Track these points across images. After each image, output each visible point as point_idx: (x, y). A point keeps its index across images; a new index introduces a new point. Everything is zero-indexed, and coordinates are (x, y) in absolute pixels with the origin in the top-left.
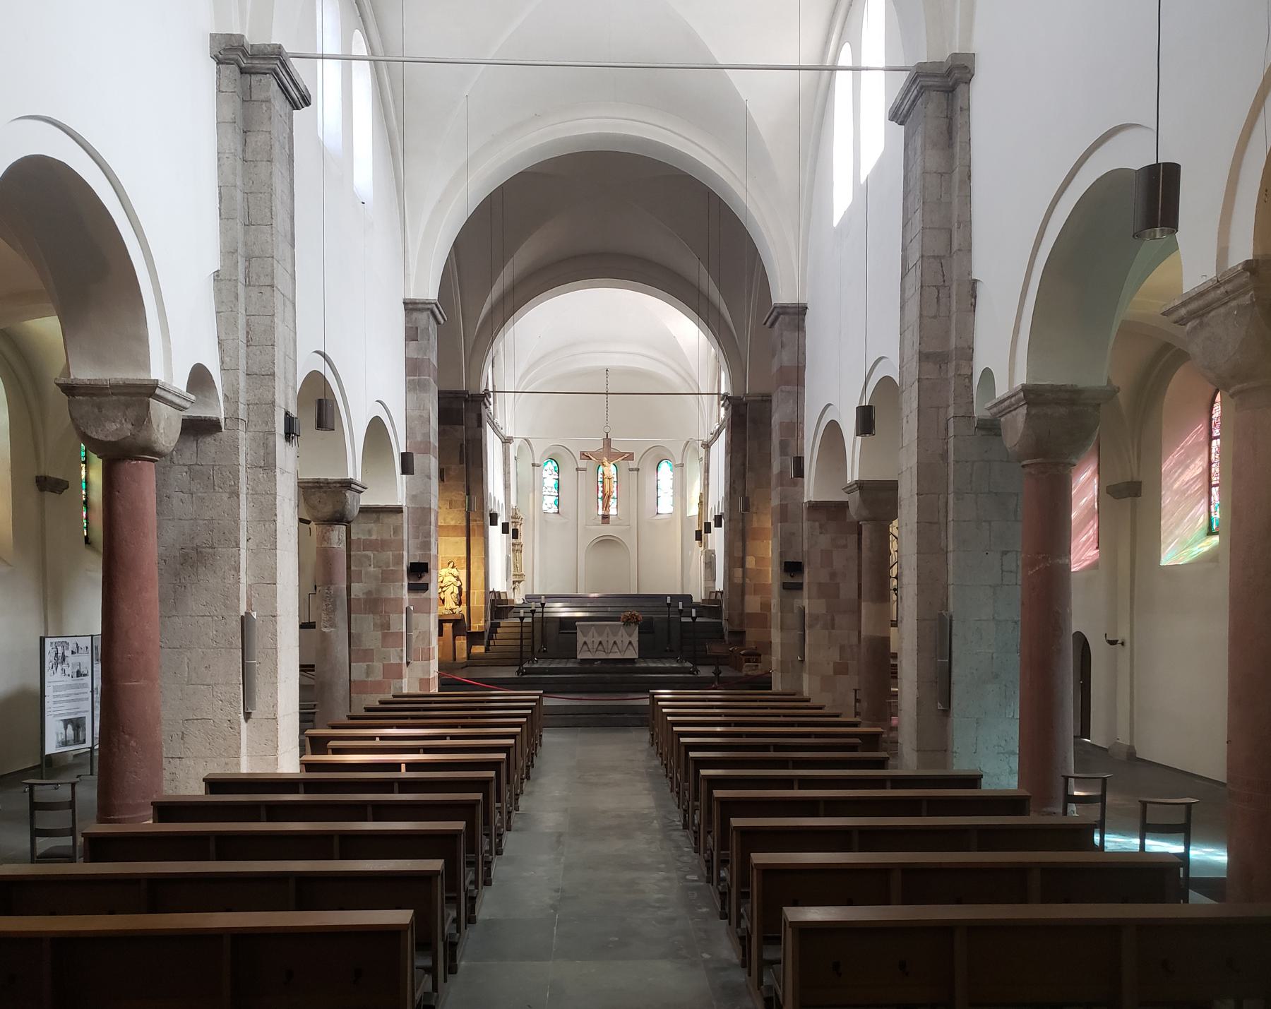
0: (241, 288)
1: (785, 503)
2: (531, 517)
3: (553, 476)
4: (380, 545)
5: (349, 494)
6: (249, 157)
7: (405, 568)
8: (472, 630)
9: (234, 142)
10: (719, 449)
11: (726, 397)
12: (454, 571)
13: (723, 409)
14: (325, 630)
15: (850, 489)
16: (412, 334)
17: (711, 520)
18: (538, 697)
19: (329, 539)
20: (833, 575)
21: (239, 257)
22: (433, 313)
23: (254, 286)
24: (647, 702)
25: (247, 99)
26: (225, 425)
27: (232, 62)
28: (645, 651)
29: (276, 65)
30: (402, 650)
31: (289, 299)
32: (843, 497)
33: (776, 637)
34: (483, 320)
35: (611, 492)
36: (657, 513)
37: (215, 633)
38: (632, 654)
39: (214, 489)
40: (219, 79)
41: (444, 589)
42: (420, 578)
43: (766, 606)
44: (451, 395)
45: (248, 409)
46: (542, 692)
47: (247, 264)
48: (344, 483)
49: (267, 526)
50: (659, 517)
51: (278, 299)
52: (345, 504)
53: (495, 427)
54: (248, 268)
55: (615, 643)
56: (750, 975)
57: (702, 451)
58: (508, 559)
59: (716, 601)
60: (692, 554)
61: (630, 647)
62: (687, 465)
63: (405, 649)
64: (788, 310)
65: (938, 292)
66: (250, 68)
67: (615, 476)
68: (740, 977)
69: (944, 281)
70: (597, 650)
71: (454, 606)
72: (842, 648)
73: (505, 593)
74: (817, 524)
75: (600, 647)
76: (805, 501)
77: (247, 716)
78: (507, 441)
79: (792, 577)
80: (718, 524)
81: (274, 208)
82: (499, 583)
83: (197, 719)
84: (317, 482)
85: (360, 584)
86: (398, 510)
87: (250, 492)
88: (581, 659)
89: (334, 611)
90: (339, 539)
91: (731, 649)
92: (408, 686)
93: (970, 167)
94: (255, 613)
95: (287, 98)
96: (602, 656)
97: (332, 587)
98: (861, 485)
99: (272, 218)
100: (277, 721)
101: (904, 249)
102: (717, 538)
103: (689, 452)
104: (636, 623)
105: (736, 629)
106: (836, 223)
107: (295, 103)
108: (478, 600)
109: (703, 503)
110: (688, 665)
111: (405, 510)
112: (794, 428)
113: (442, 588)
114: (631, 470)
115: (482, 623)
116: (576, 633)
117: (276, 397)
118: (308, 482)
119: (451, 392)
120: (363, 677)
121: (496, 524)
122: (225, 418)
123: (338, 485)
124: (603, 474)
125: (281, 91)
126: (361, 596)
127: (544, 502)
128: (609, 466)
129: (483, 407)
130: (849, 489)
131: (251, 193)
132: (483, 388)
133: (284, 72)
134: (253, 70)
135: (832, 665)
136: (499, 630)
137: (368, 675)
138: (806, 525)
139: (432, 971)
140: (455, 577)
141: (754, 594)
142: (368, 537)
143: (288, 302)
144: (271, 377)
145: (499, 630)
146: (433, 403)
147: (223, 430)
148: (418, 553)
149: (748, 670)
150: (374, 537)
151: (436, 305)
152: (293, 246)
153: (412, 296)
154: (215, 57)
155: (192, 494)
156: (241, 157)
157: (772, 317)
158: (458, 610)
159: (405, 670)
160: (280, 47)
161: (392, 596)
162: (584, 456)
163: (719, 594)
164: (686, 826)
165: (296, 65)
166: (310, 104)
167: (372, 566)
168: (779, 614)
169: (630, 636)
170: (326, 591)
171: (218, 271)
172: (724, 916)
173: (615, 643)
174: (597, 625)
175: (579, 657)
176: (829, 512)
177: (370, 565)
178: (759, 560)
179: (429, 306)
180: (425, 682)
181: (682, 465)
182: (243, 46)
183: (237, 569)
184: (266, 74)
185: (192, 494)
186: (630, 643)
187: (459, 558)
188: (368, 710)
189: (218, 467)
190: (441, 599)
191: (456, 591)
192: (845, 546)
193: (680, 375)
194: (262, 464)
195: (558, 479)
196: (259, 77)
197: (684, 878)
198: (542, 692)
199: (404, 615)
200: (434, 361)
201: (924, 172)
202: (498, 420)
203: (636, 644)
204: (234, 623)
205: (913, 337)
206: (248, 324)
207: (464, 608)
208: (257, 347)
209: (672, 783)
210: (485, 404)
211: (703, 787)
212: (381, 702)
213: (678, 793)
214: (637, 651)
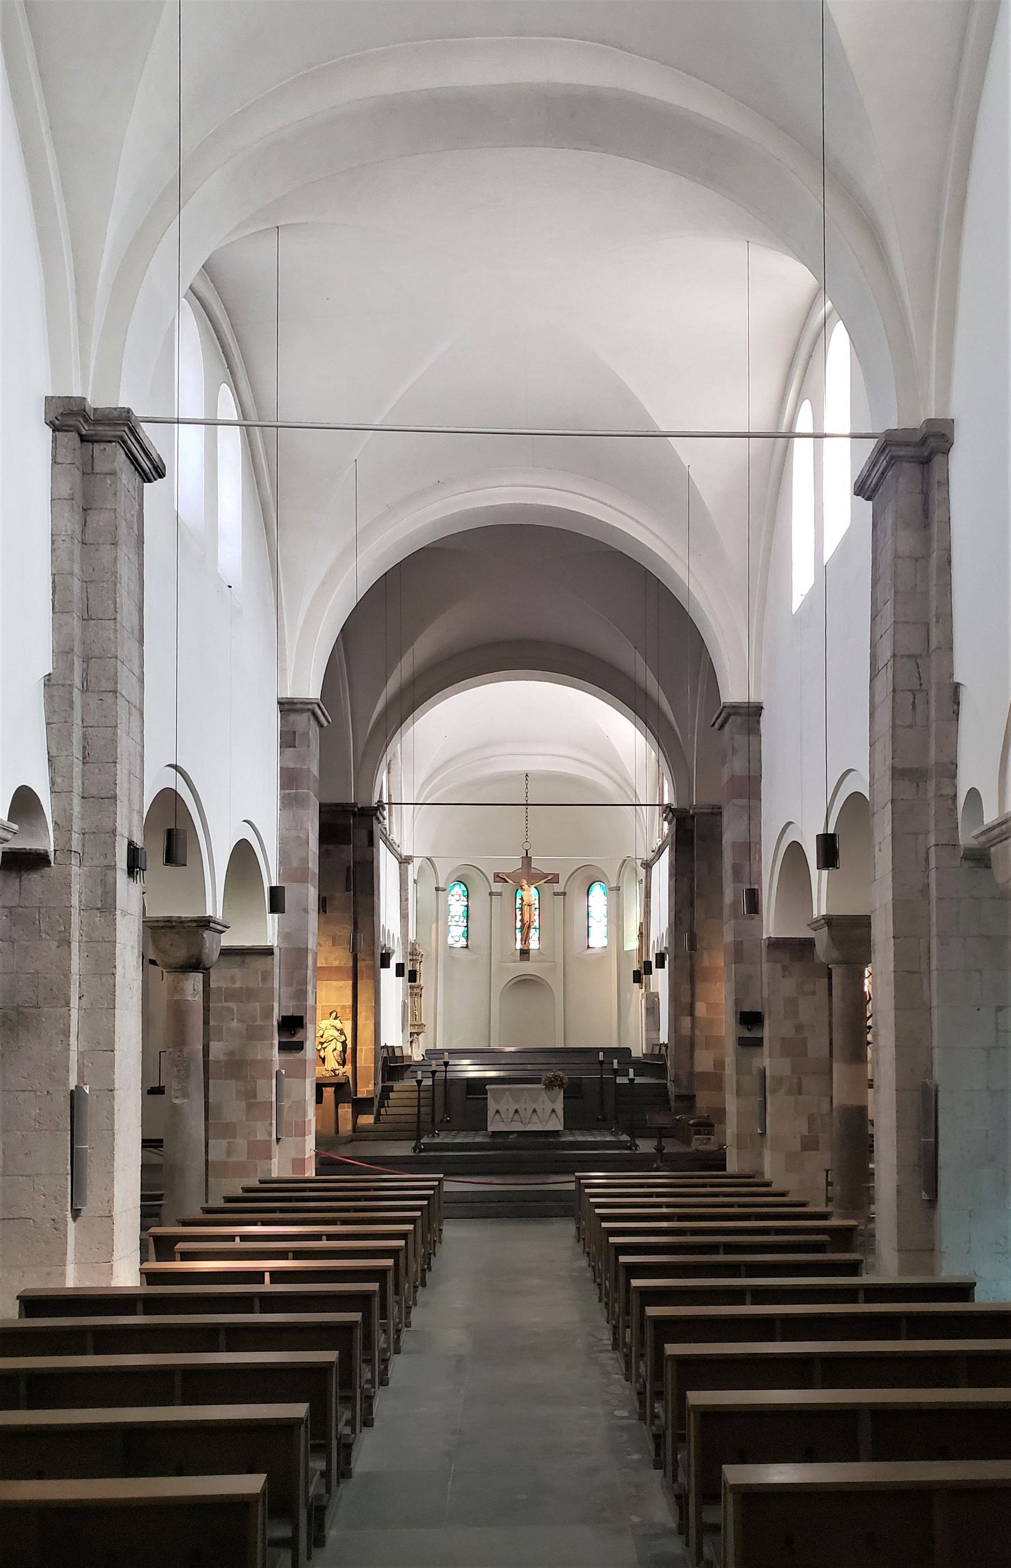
0: (77, 694)
1: (740, 939)
2: (434, 955)
3: (460, 903)
4: (246, 995)
5: (207, 934)
6: (89, 539)
7: (275, 1023)
8: (359, 1096)
9: (71, 523)
11: (668, 808)
12: (337, 1023)
13: (666, 823)
14: (176, 1101)
15: (816, 925)
16: (288, 740)
17: (652, 959)
18: (436, 1183)
19: (182, 990)
20: (799, 1028)
21: (75, 658)
22: (314, 714)
23: (93, 692)
24: (572, 1187)
25: (88, 471)
26: (55, 858)
27: (72, 428)
28: (571, 1120)
29: (124, 432)
30: (271, 1124)
31: (135, 707)
32: (809, 934)
33: (731, 1105)
34: (374, 723)
35: (531, 922)
36: (588, 947)
37: (38, 1111)
38: (556, 1124)
39: (41, 936)
40: (55, 448)
41: (324, 1046)
42: (293, 1035)
43: (719, 1064)
44: (338, 809)
45: (83, 839)
46: (442, 1176)
47: (85, 666)
48: (201, 921)
49: (104, 980)
50: (590, 951)
51: (122, 707)
52: (202, 948)
53: (390, 846)
54: (85, 672)
55: (534, 1111)
56: (687, 1545)
57: (642, 872)
58: (404, 1005)
59: (660, 1056)
60: (631, 997)
61: (553, 1116)
62: (624, 888)
63: (274, 1122)
64: (741, 711)
65: (914, 697)
66: (92, 435)
67: (537, 902)
68: (675, 1546)
69: (921, 684)
70: (512, 1121)
71: (337, 1066)
72: (811, 1119)
73: (401, 1047)
74: (779, 966)
75: (517, 1117)
76: (765, 937)
77: (76, 1214)
78: (404, 861)
79: (749, 1030)
80: (660, 964)
81: (118, 600)
82: (392, 1035)
83: (14, 1219)
84: (169, 921)
85: (222, 1042)
86: (268, 952)
87: (85, 939)
88: (492, 1132)
89: (187, 1077)
90: (194, 990)
91: (677, 1118)
92: (278, 1168)
93: (950, 550)
94: (88, 1087)
95: (136, 469)
97: (186, 1050)
98: (830, 921)
99: (117, 612)
100: (113, 1220)
101: (873, 646)
102: (660, 980)
103: (627, 873)
104: (560, 1086)
105: (684, 1092)
106: (797, 603)
107: (146, 475)
108: (366, 1058)
109: (643, 934)
110: (625, 1138)
111: (276, 951)
112: (749, 849)
113: (322, 1043)
114: (556, 894)
115: (371, 1087)
116: (486, 1098)
117: (118, 824)
118: (158, 921)
119: (337, 805)
120: (223, 1157)
121: (388, 966)
122: (55, 851)
123: (194, 924)
124: (522, 899)
125: (129, 461)
126: (222, 1057)
127: (450, 935)
128: (530, 891)
129: (375, 822)
130: (815, 925)
131: (91, 582)
132: (376, 799)
133: (133, 440)
134: (95, 438)
135: (798, 1138)
136: (392, 1095)
137: (229, 1154)
138: (765, 966)
139: (291, 1543)
140: (338, 1030)
141: (706, 1049)
142: (229, 985)
143: (134, 710)
144: (113, 801)
145: (392, 1095)
146: (312, 821)
147: (52, 864)
148: (291, 1003)
149: (698, 1144)
150: (237, 985)
151: (319, 706)
152: (141, 642)
153: (289, 694)
154: (51, 424)
155: (13, 942)
156: (80, 540)
157: (721, 718)
158: (341, 1071)
159: (275, 1148)
160: (129, 410)
161: (259, 1057)
162: (499, 878)
163: (663, 1048)
164: (615, 1347)
165: (147, 430)
166: (164, 476)
167: (235, 1021)
168: (735, 1076)
169: (553, 1102)
170: (178, 1053)
171: (49, 674)
172: (658, 1465)
173: (534, 1111)
174: (514, 1089)
175: (490, 1129)
177: (233, 1020)
178: (711, 1007)
179: (310, 707)
180: (299, 1163)
181: (618, 889)
182: (84, 410)
183: (67, 1034)
184: (110, 442)
185: (13, 942)
186: (553, 1111)
187: (344, 1007)
188: (228, 1200)
189: (45, 910)
190: (320, 1057)
191: (340, 1047)
192: (813, 993)
193: (615, 781)
194: (99, 906)
195: (467, 906)
196: (102, 446)
197: (611, 1414)
198: (442, 1176)
199: (274, 1081)
200: (315, 770)
201: (897, 557)
202: (395, 836)
203: (560, 1112)
204: (62, 1099)
205: (885, 748)
206: (85, 737)
207: (348, 1067)
208: (95, 765)
209: (601, 1290)
210: (378, 819)
211: (635, 1299)
212: (246, 1190)
213: (607, 1304)
214: (562, 1121)
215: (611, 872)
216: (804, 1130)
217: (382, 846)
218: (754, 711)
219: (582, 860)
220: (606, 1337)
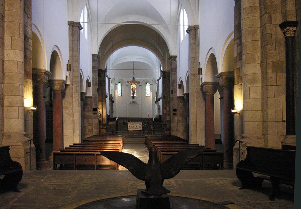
10: (161, 81)
57: (157, 82)
74: (179, 101)
101: (189, 55)
102: (160, 103)
112: (175, 81)
114: (139, 85)
115: (105, 122)
153: (93, 53)
207: (101, 118)
218: (175, 57)
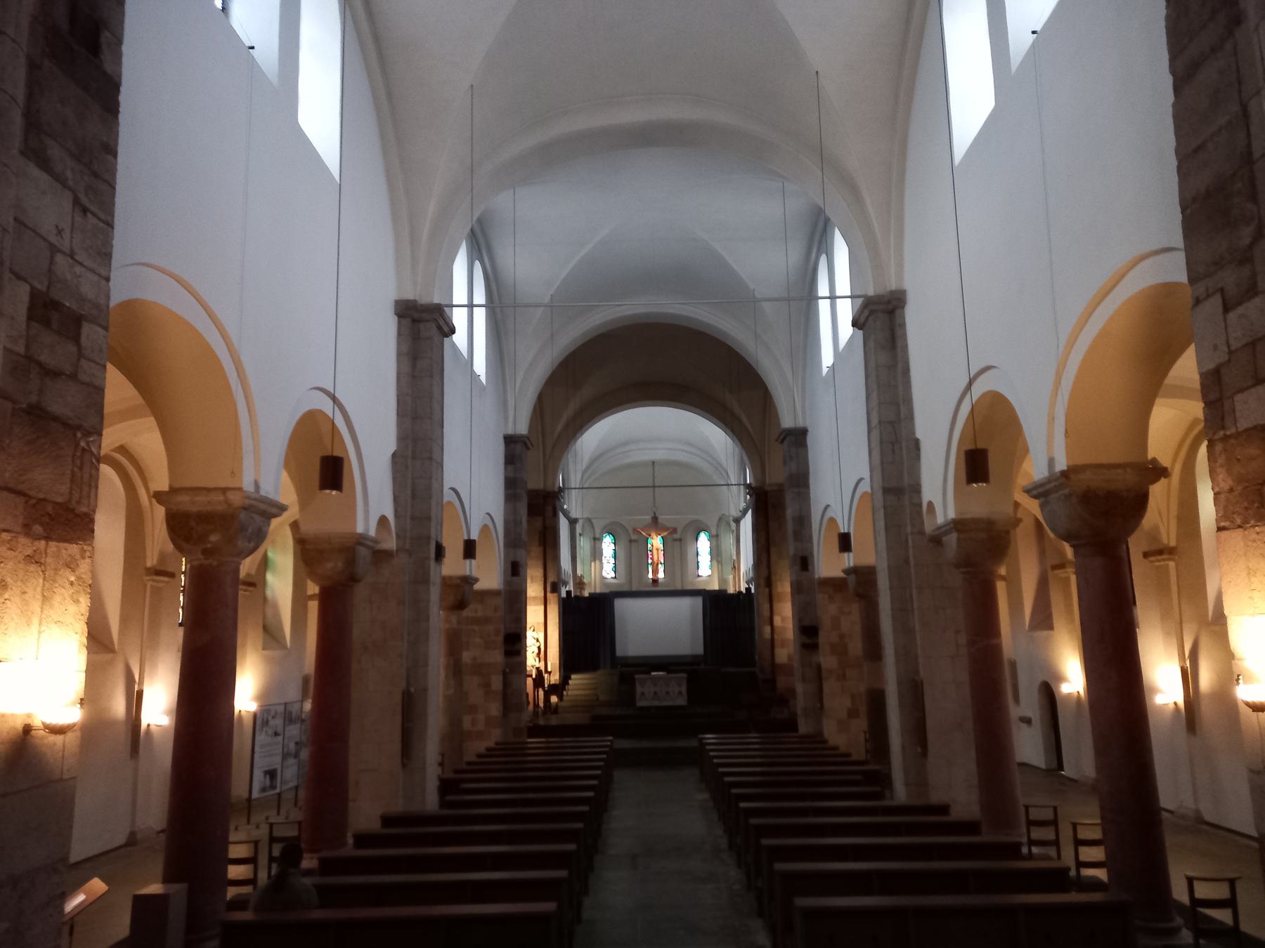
11: (749, 487)
13: (748, 497)
20: (842, 637)
33: (800, 688)
36: (699, 576)
38: (682, 701)
46: (611, 738)
50: (699, 579)
57: (733, 525)
78: (573, 522)
96: (656, 703)
114: (675, 540)
132: (557, 486)
145: (570, 682)
173: (667, 693)
176: (834, 585)
178: (783, 619)
181: (717, 536)
186: (680, 693)
187: (539, 623)
191: (537, 651)
195: (615, 550)
215: (712, 522)
216: (848, 703)
217: (561, 514)
219: (691, 517)
220: (724, 842)
